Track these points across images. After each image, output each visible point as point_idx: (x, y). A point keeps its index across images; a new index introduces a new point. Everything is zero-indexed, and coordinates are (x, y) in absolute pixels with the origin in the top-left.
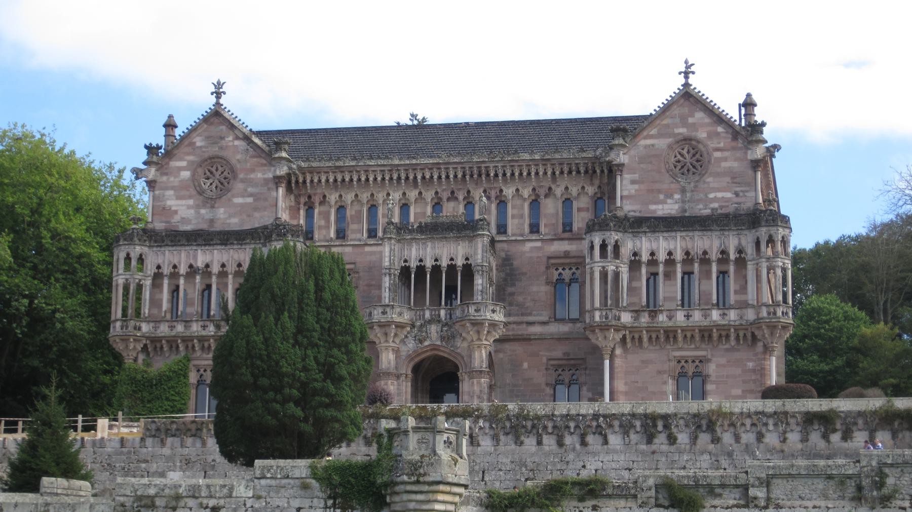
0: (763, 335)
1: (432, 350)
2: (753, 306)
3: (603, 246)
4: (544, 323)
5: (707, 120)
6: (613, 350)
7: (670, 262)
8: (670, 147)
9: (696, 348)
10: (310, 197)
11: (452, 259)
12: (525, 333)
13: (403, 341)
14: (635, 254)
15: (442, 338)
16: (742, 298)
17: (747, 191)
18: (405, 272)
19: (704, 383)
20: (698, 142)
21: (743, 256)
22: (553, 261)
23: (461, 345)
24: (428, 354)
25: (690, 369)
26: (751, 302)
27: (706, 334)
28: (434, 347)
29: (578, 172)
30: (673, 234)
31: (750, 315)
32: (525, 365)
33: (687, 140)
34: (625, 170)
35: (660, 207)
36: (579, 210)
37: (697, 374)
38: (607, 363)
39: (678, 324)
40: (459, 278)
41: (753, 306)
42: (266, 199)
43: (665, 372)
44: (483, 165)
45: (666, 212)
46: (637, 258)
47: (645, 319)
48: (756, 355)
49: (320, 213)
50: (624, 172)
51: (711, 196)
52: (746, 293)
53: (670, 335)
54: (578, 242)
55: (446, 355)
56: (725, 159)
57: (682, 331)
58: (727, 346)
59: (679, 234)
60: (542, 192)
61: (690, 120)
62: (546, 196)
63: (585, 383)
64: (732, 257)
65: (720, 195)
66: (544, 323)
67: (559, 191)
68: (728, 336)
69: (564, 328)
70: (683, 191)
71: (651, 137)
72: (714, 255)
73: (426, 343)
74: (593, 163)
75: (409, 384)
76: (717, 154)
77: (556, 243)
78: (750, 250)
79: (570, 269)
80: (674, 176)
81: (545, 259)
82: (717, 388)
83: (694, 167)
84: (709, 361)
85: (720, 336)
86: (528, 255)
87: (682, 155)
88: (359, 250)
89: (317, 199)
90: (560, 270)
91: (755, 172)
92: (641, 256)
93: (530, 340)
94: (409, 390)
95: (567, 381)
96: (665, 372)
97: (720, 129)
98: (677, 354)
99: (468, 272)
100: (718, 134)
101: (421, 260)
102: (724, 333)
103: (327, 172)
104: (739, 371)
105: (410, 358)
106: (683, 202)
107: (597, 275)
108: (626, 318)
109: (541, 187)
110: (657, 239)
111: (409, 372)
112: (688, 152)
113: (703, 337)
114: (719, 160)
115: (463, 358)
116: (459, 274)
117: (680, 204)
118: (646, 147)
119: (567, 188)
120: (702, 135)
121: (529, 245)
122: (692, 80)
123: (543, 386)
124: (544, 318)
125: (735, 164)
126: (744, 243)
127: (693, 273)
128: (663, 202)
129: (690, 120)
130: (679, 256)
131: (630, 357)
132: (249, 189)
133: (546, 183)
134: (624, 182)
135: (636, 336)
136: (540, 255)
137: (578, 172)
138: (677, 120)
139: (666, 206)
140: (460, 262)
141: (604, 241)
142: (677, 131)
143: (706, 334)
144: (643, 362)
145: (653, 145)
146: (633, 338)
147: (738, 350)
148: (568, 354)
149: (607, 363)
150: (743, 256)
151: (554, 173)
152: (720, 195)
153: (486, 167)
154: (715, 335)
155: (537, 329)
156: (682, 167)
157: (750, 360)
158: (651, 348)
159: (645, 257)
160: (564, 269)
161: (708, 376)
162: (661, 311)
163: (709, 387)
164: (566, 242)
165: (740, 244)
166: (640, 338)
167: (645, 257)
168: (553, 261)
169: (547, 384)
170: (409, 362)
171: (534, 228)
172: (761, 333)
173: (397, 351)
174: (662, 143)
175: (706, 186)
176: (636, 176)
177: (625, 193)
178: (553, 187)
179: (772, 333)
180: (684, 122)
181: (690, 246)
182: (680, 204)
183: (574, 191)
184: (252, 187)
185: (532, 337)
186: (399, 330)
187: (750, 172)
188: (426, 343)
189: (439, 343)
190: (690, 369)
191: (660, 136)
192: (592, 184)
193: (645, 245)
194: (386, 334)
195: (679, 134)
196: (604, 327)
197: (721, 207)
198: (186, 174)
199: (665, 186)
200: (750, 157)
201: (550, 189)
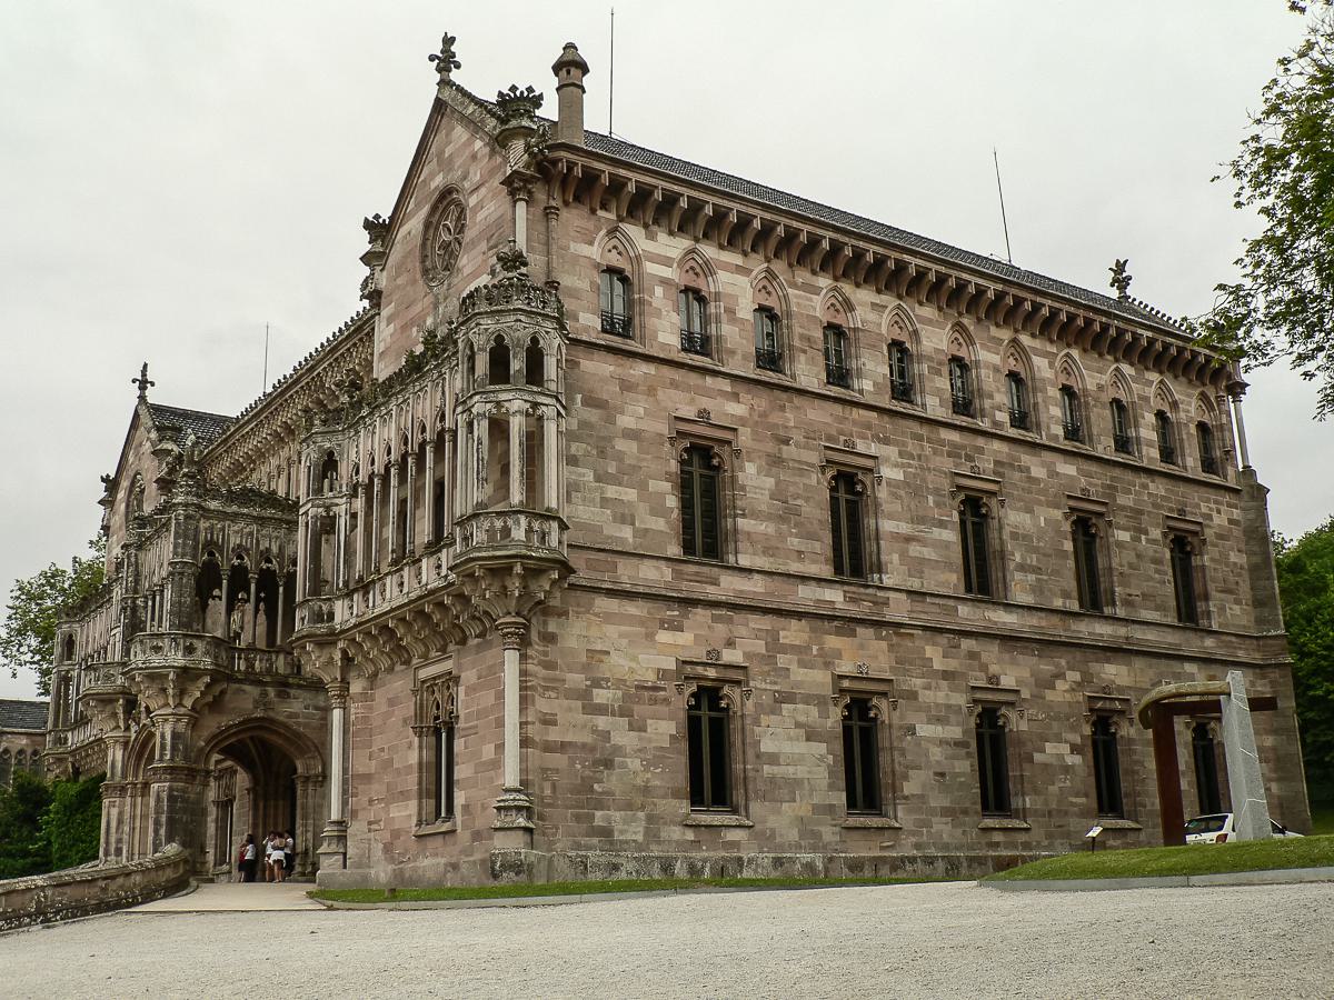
8: (427, 225)
191: (418, 206)
198: (123, 506)
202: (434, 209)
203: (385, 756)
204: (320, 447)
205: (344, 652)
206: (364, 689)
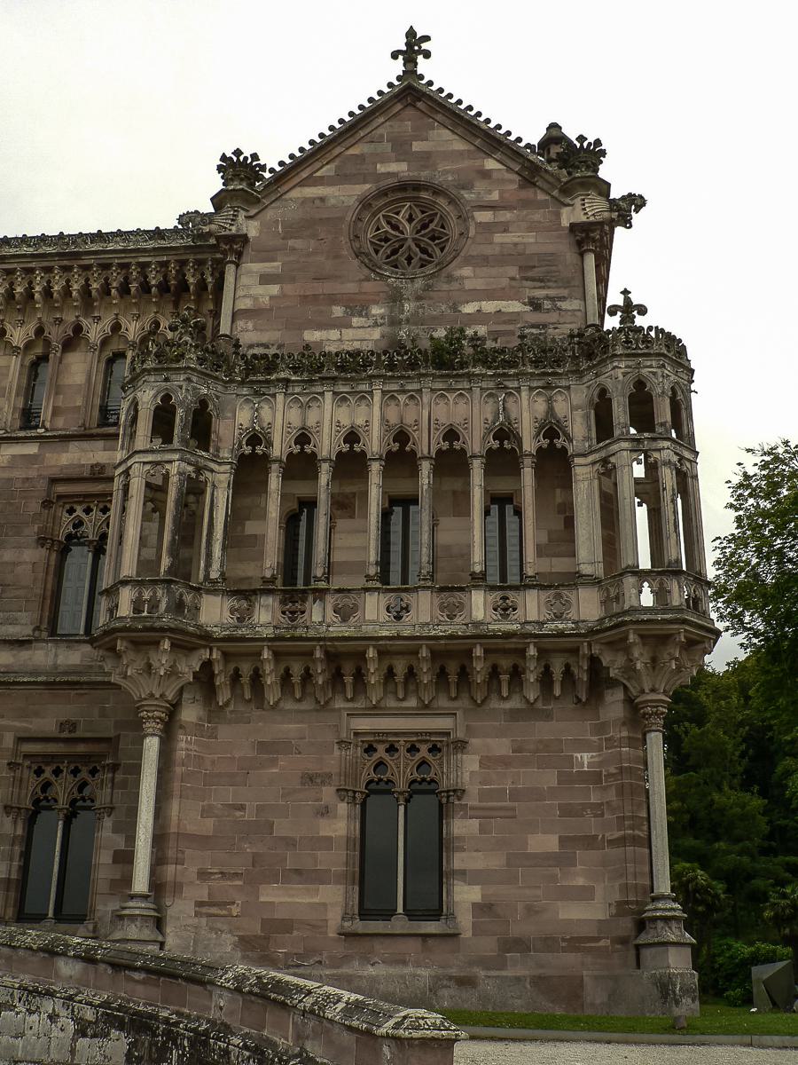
0: (629, 669)
2: (595, 582)
5: (460, 145)
6: (174, 709)
7: (351, 463)
8: (365, 203)
9: (425, 709)
14: (254, 440)
16: (560, 565)
17: (563, 299)
19: (442, 813)
20: (437, 191)
21: (559, 443)
22: (61, 489)
25: (402, 771)
26: (586, 569)
27: (453, 668)
29: (145, 287)
30: (364, 387)
31: (588, 607)
33: (406, 189)
34: (249, 252)
35: (334, 334)
37: (424, 787)
38: (152, 746)
39: (368, 630)
41: (595, 582)
43: (326, 778)
45: (348, 347)
46: (259, 450)
47: (266, 615)
48: (601, 728)
51: (469, 309)
52: (573, 554)
53: (343, 665)
56: (505, 228)
57: (382, 653)
58: (515, 703)
59: (378, 387)
60: (56, 334)
61: (417, 146)
62: (69, 345)
64: (529, 445)
65: (489, 307)
68: (517, 674)
70: (395, 298)
71: (321, 181)
72: (476, 442)
76: (484, 217)
78: (579, 429)
80: (373, 267)
81: (42, 485)
82: (482, 830)
83: (424, 251)
84: (461, 746)
85: (494, 673)
87: (395, 227)
90: (79, 511)
91: (582, 255)
92: (270, 444)
95: (63, 802)
96: (326, 778)
97: (491, 164)
98: (364, 724)
100: (486, 175)
102: (505, 663)
104: (549, 779)
106: (394, 322)
107: (137, 486)
108: (214, 613)
110: (316, 398)
112: (410, 220)
113: (442, 675)
114: (488, 228)
117: (386, 329)
118: (305, 201)
119: (116, 327)
120: (444, 174)
122: (423, 66)
125: (530, 238)
126: (561, 408)
127: (415, 501)
128: (342, 324)
129: (417, 146)
130: (374, 443)
131: (225, 732)
133: (70, 318)
134: (244, 280)
135: (246, 669)
136: (32, 473)
137: (145, 287)
138: (387, 147)
139: (348, 334)
141: (167, 398)
142: (381, 168)
143: (453, 668)
144: (263, 747)
145: (322, 199)
146: (236, 677)
147: (548, 716)
148: (73, 726)
149: (152, 746)
150: (559, 443)
151: (86, 291)
152: (489, 307)
154: (480, 667)
156: (395, 252)
157: (584, 746)
158: (289, 705)
159: (280, 447)
161: (459, 792)
162: (320, 594)
163: (461, 827)
164: (100, 444)
165: (550, 410)
166: (257, 677)
167: (280, 447)
168: (61, 489)
171: (28, 417)
172: (621, 660)
174: (345, 196)
175: (455, 286)
176: (274, 267)
177: (241, 305)
178: (85, 322)
179: (654, 660)
180: (401, 149)
181: (409, 420)
182: (386, 329)
187: (570, 256)
190: (402, 771)
191: (341, 178)
193: (280, 418)
195: (389, 174)
196: (143, 638)
197: (495, 336)
199: (351, 287)
200: (565, 223)
201: (78, 329)
202: (383, 193)
203: (248, 816)
204: (195, 388)
205: (207, 665)
206: (200, 719)
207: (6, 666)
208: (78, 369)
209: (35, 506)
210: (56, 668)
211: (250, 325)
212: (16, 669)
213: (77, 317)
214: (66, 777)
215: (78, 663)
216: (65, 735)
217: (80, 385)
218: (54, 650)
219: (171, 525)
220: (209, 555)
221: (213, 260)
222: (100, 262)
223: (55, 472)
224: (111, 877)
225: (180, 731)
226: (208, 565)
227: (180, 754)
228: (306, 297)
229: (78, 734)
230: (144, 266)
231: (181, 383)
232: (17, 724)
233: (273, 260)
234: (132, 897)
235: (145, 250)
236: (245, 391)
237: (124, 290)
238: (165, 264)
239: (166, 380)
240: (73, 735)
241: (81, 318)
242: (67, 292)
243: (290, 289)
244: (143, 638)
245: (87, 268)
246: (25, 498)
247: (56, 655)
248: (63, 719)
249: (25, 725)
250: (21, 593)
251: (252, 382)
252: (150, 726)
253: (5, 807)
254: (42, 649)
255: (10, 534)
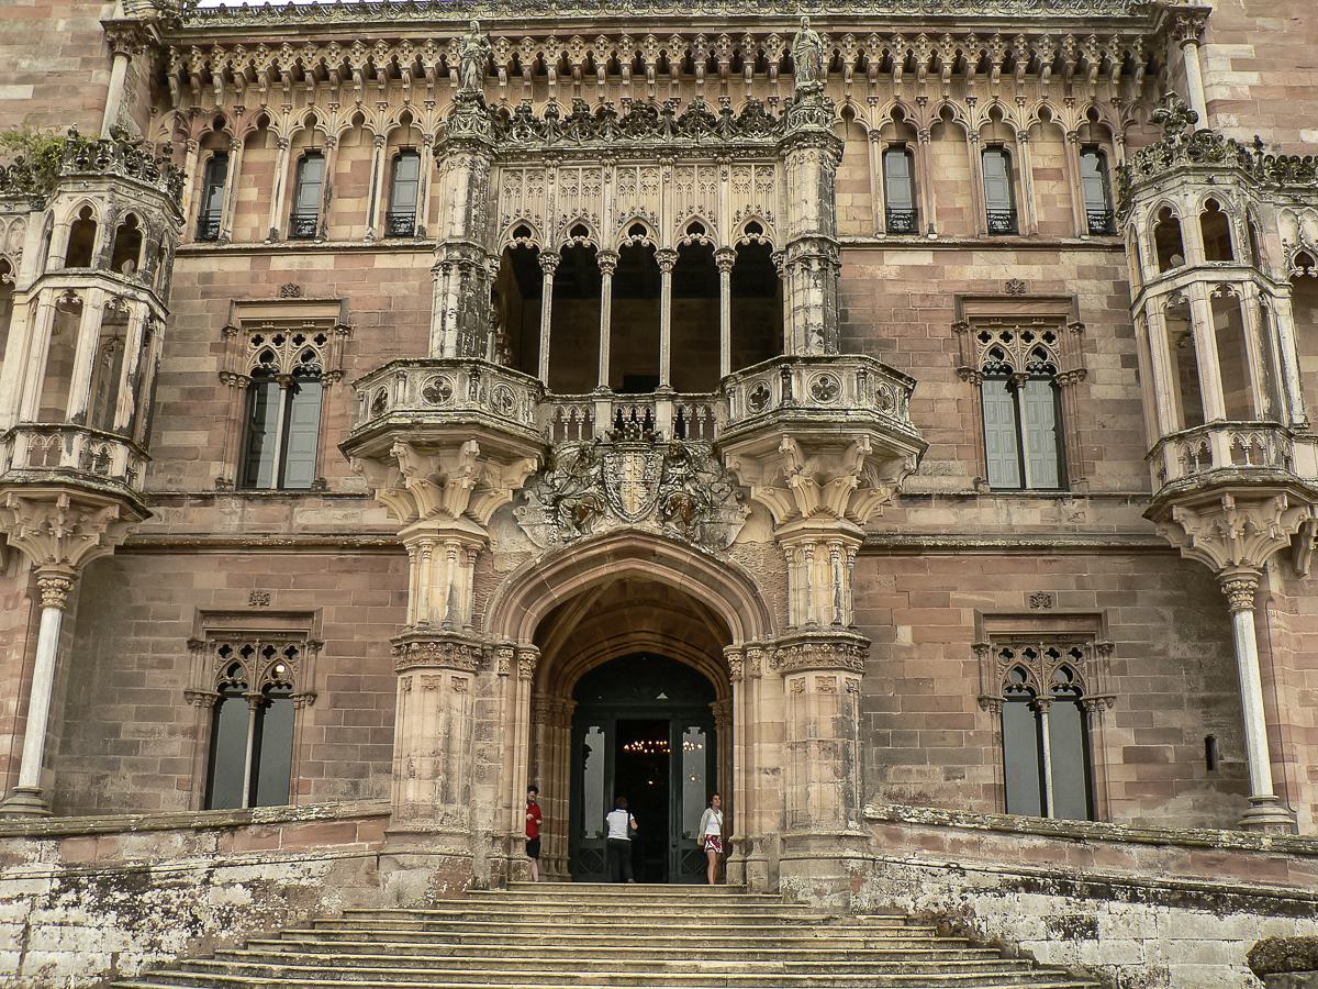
1: (619, 554)
3: (1213, 219)
4: (961, 498)
10: (219, 122)
11: (696, 227)
12: (899, 528)
13: (500, 515)
15: (669, 508)
18: (522, 263)
22: (973, 309)
23: (747, 540)
24: (606, 569)
28: (633, 546)
29: (1033, 68)
32: (905, 634)
36: (1038, 174)
38: (1245, 622)
40: (725, 291)
42: (74, 91)
44: (749, 31)
49: (244, 168)
50: (1207, 37)
54: (1048, 256)
55: (676, 577)
62: (936, 132)
63: (1110, 700)
66: (961, 498)
67: (974, 116)
69: (1030, 517)
73: (603, 526)
74: (1080, 39)
75: (525, 689)
77: (978, 256)
79: (1028, 337)
86: (898, 289)
88: (353, 264)
89: (238, 127)
93: (918, 549)
94: (524, 711)
99: (758, 272)
101: (580, 230)
103: (275, 46)
105: (531, 583)
109: (921, 102)
111: (526, 642)
115: (751, 586)
116: (725, 278)
119: (995, 113)
121: (894, 261)
123: (970, 706)
124: (963, 484)
131: (1306, 605)
132: (24, 64)
133: (935, 97)
134: (1213, 64)
136: (932, 289)
137: (1033, 68)
140: (726, 236)
141: (1212, 205)
151: (959, 67)
153: (760, 38)
155: (933, 518)
160: (1006, 337)
164: (1011, 256)
168: (973, 309)
169: (982, 701)
170: (527, 601)
173: (479, 555)
176: (1245, 50)
177: (1221, 94)
178: (958, 105)
183: (1021, 116)
184: (36, 56)
185: (925, 542)
186: (493, 467)
188: (603, 526)
189: (652, 525)
192: (1070, 102)
194: (441, 483)
196: (1255, 493)
201: (946, 112)
207: (948, 527)
208: (946, 161)
209: (943, 330)
210: (1012, 530)
211: (1233, 120)
212: (961, 530)
213: (945, 97)
214: (1044, 659)
215: (1039, 523)
216: (1041, 610)
217: (956, 182)
218: (1005, 508)
219: (1260, 359)
220: (1288, 396)
221: (1122, 38)
222: (978, 31)
223: (964, 290)
224: (1124, 780)
225: (1270, 604)
226: (1290, 408)
227: (1274, 632)
228: (1294, 88)
229: (1055, 610)
230: (1031, 39)
231: (1229, 187)
232: (975, 597)
233: (1242, 41)
234: (1259, 802)
235: (1036, 20)
236: (1281, 200)
237: (1008, 67)
238: (1057, 39)
239: (1210, 181)
240: (1048, 611)
241: (950, 99)
242: (934, 67)
243: (1271, 78)
244: (1255, 493)
245: (958, 37)
246: (929, 319)
247: (1009, 514)
248: (1034, 592)
249: (982, 598)
250: (949, 436)
251: (1291, 189)
252: (1245, 599)
253: (980, 700)
254: (991, 506)
255: (920, 363)
